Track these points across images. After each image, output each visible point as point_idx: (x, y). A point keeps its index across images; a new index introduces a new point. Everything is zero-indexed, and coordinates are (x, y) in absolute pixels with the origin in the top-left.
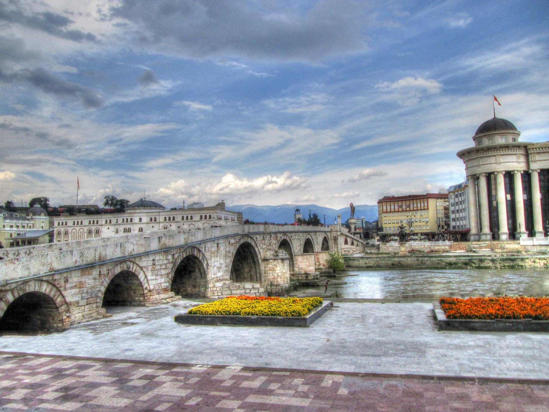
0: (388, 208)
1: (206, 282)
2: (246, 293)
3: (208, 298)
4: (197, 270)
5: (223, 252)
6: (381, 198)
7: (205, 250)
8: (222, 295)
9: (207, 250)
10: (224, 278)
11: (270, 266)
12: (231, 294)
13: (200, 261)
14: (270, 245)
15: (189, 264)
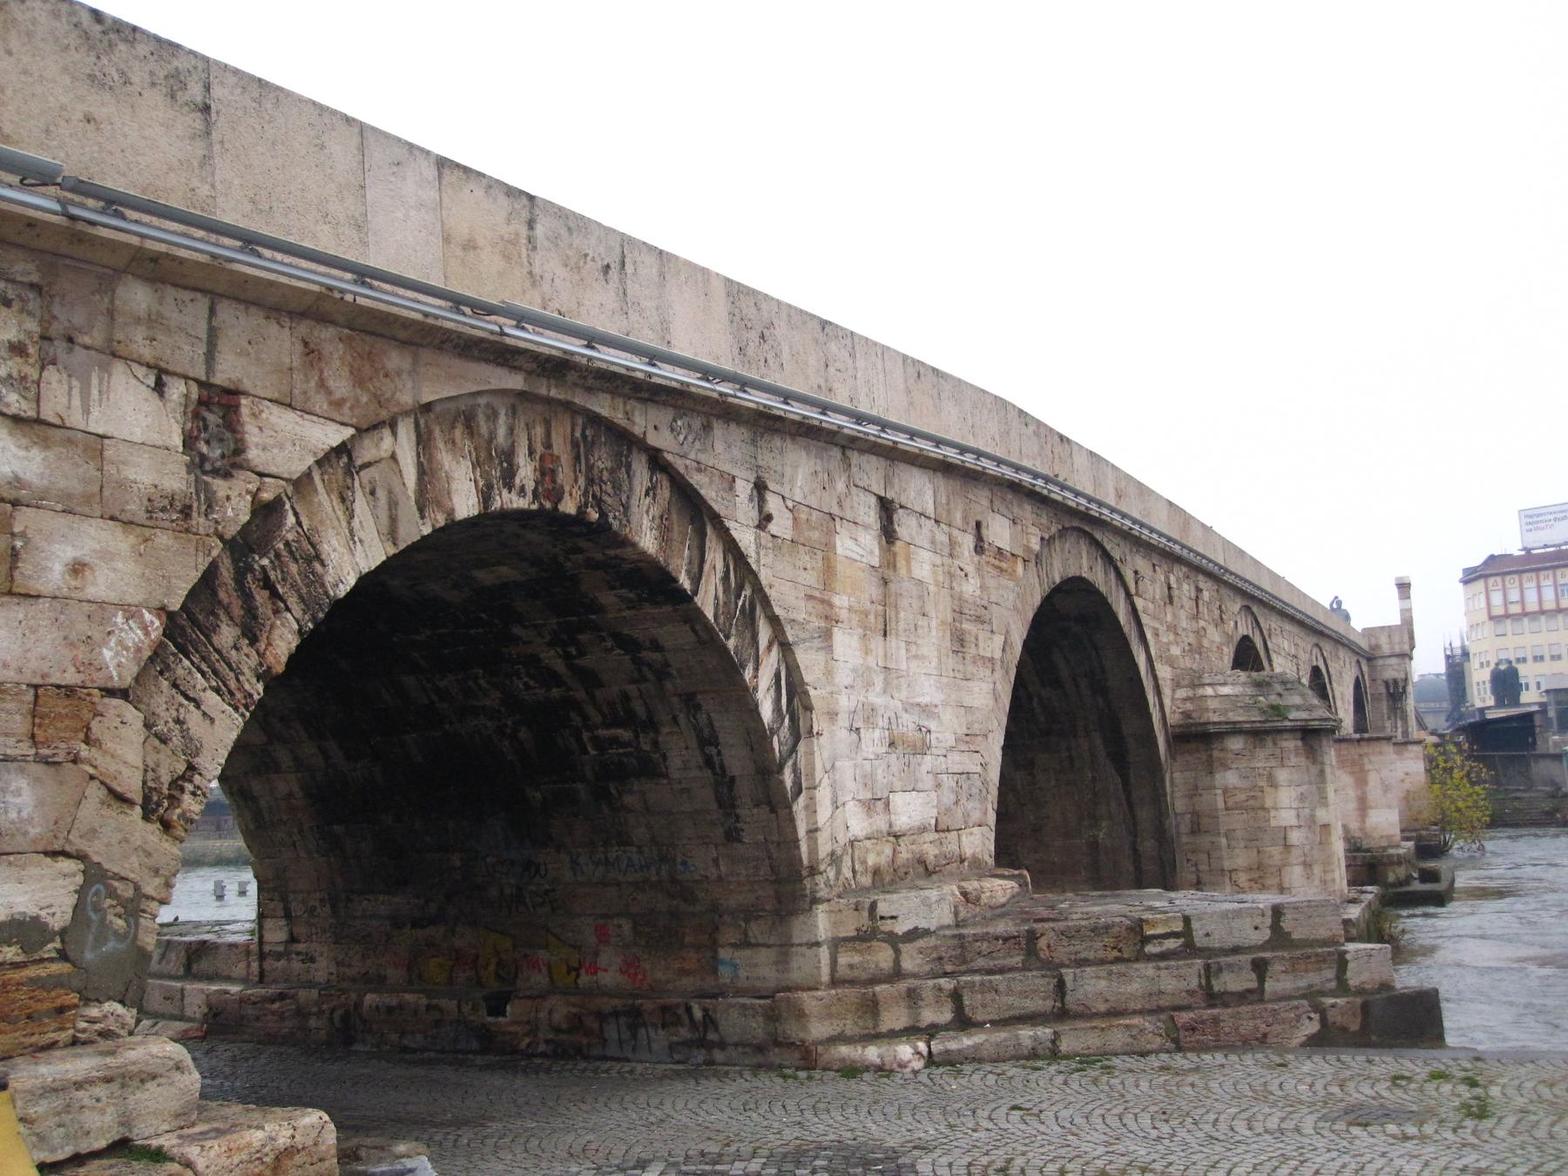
0: (1514, 596)
1: (786, 885)
2: (1213, 998)
3: (808, 1059)
4: (679, 753)
5: (940, 610)
6: (1477, 560)
7: (765, 519)
8: (963, 1022)
9: (781, 525)
10: (951, 844)
11: (1230, 778)
12: (1062, 1014)
13: (707, 639)
14: (1201, 646)
15: (591, 680)
